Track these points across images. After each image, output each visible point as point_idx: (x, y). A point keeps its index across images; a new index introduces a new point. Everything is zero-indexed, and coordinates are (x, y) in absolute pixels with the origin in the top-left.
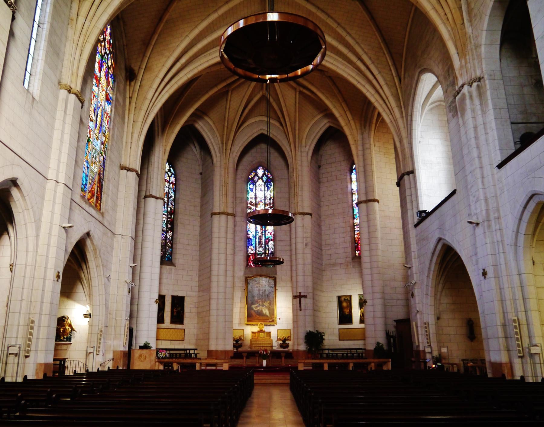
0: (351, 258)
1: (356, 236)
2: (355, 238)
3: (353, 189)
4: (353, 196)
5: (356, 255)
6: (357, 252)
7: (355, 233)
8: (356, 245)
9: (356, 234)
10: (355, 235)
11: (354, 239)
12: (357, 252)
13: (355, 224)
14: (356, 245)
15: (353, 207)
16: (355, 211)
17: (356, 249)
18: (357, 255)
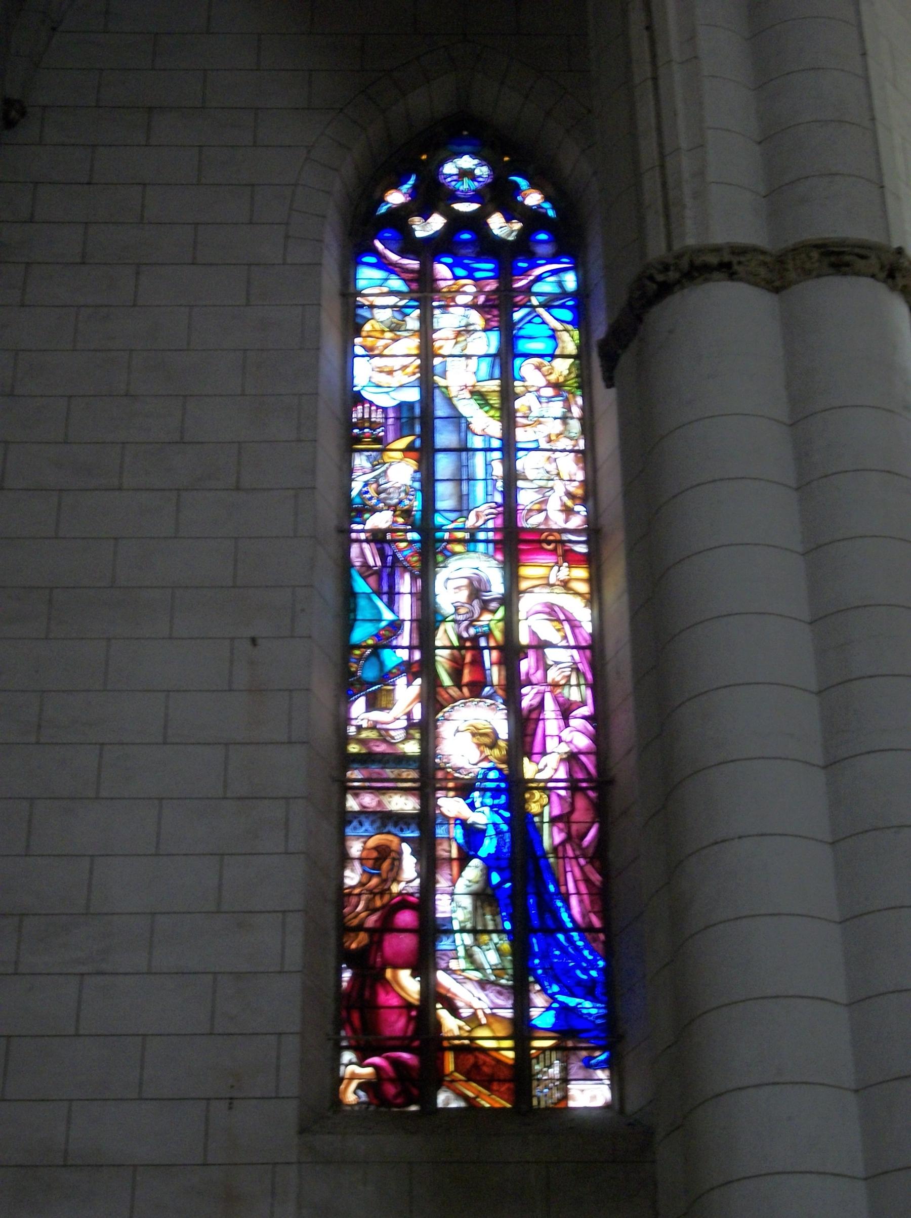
0: (290, 1111)
1: (352, 877)
2: (342, 895)
3: (359, 399)
4: (360, 461)
5: (337, 1101)
6: (348, 1056)
7: (342, 841)
8: (347, 975)
9: (356, 848)
10: (344, 859)
11: (331, 895)
12: (348, 1056)
13: (354, 748)
14: (347, 975)
15: (346, 564)
16: (364, 609)
17: (339, 1024)
18: (351, 1095)
